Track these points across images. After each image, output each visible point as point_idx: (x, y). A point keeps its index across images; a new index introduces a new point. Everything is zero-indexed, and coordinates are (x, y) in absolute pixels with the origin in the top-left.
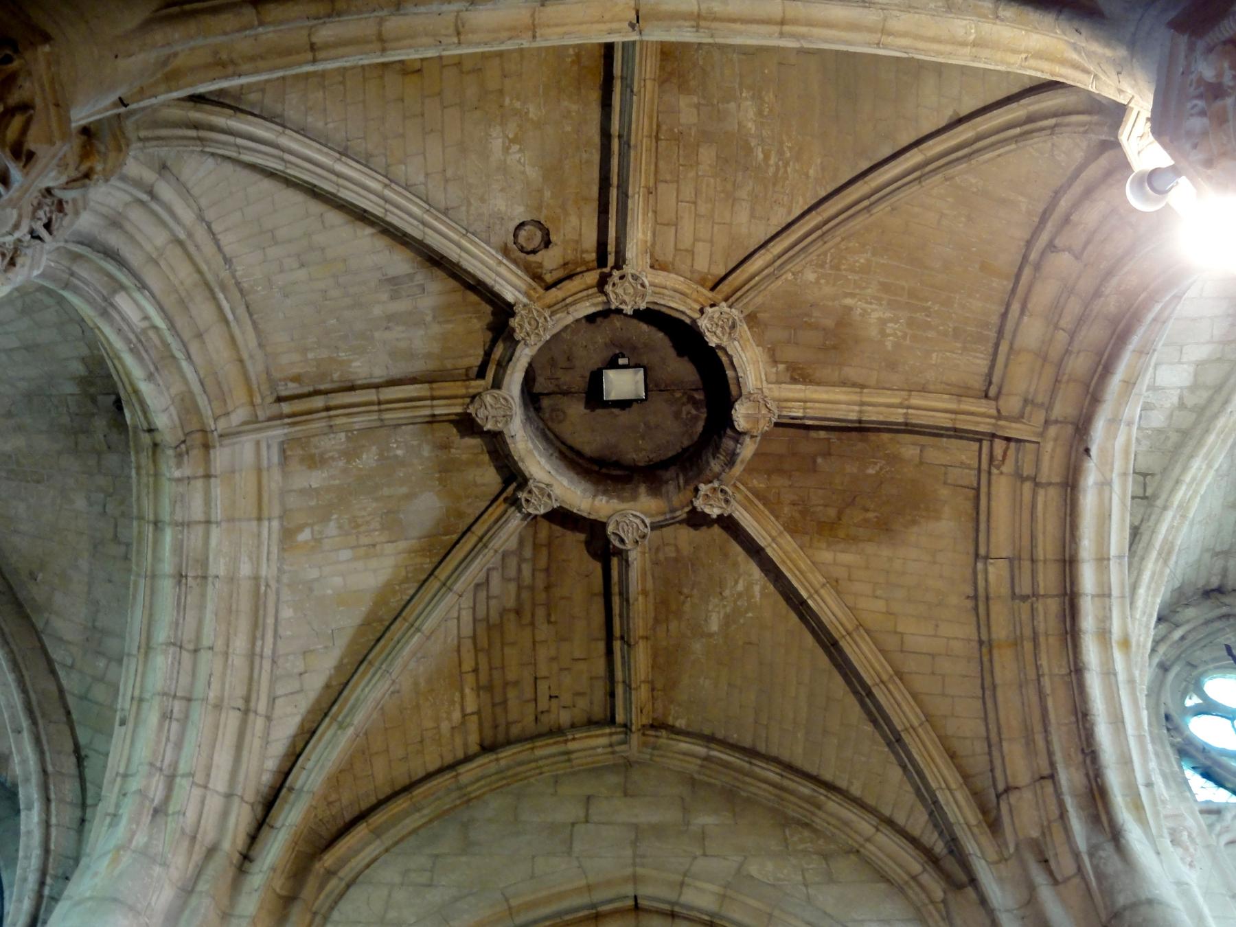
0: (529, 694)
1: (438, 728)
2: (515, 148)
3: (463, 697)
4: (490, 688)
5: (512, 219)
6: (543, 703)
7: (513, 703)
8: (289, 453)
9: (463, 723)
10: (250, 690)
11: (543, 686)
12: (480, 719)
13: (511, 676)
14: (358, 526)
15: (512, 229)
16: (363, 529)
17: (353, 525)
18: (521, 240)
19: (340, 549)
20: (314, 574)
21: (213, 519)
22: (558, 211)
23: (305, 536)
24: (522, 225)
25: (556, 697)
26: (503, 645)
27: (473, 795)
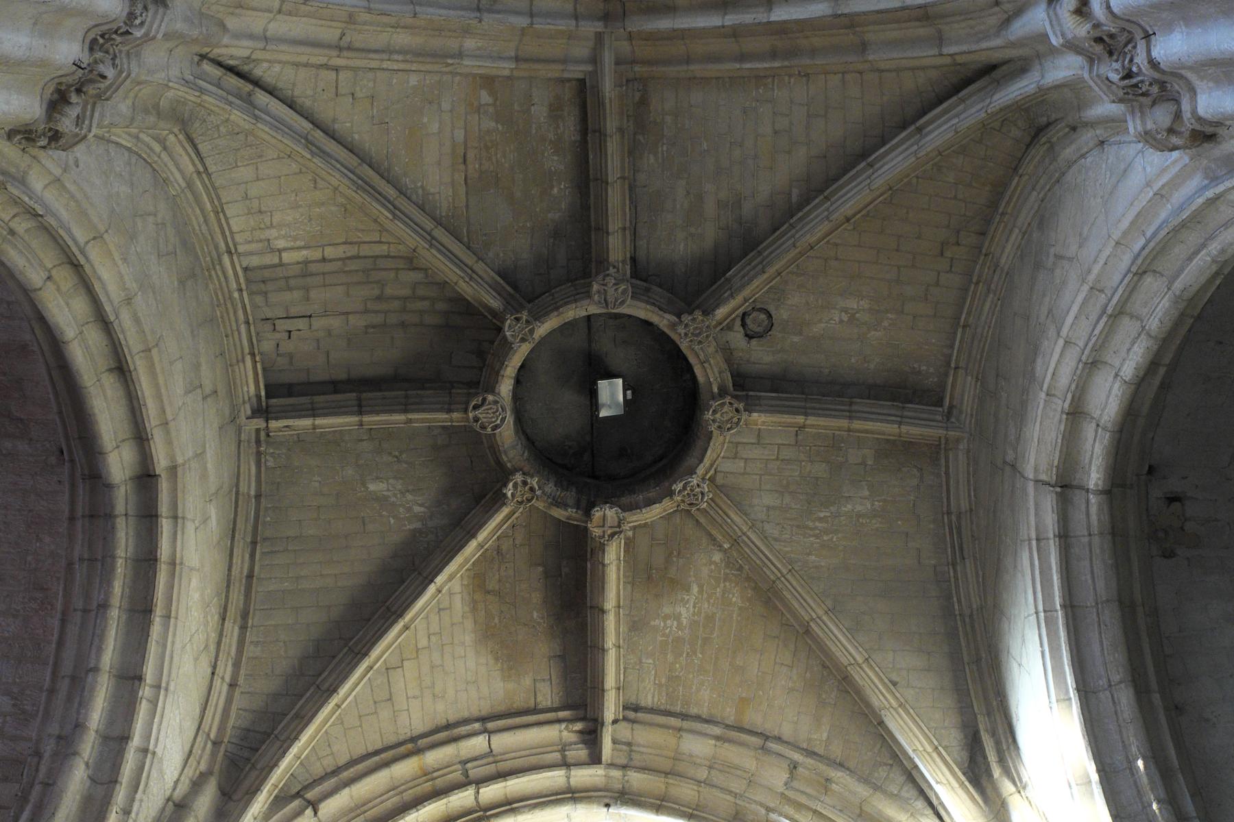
0: (294, 311)
1: (271, 226)
2: (845, 318)
3: (299, 248)
4: (305, 275)
6: (283, 325)
7: (287, 296)
8: (567, 85)
9: (272, 251)
10: (358, 50)
11: (301, 324)
12: (275, 266)
13: (313, 294)
14: (487, 148)
17: (489, 144)
19: (466, 131)
20: (446, 106)
21: (536, 20)
22: (779, 347)
23: (485, 97)
24: (770, 316)
25: (289, 337)
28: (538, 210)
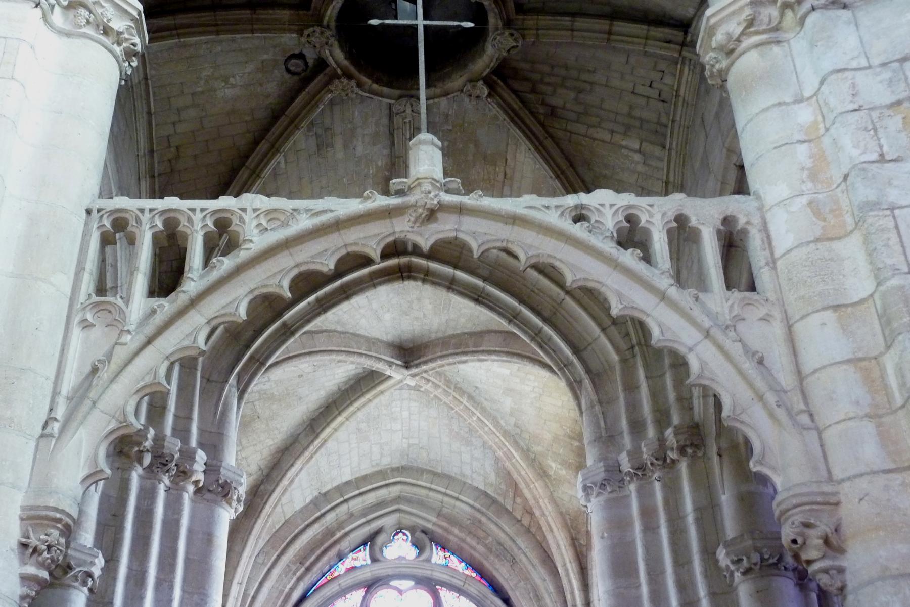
0: (642, 101)
1: (639, 173)
2: (232, 80)
3: (626, 148)
4: (628, 128)
5: (283, 76)
7: (645, 114)
11: (640, 90)
13: (625, 109)
14: (489, 179)
15: (290, 76)
16: (492, 177)
17: (488, 182)
18: (299, 70)
22: (277, 49)
25: (651, 82)
26: (601, 108)
27: (680, 183)
28: (459, 134)
